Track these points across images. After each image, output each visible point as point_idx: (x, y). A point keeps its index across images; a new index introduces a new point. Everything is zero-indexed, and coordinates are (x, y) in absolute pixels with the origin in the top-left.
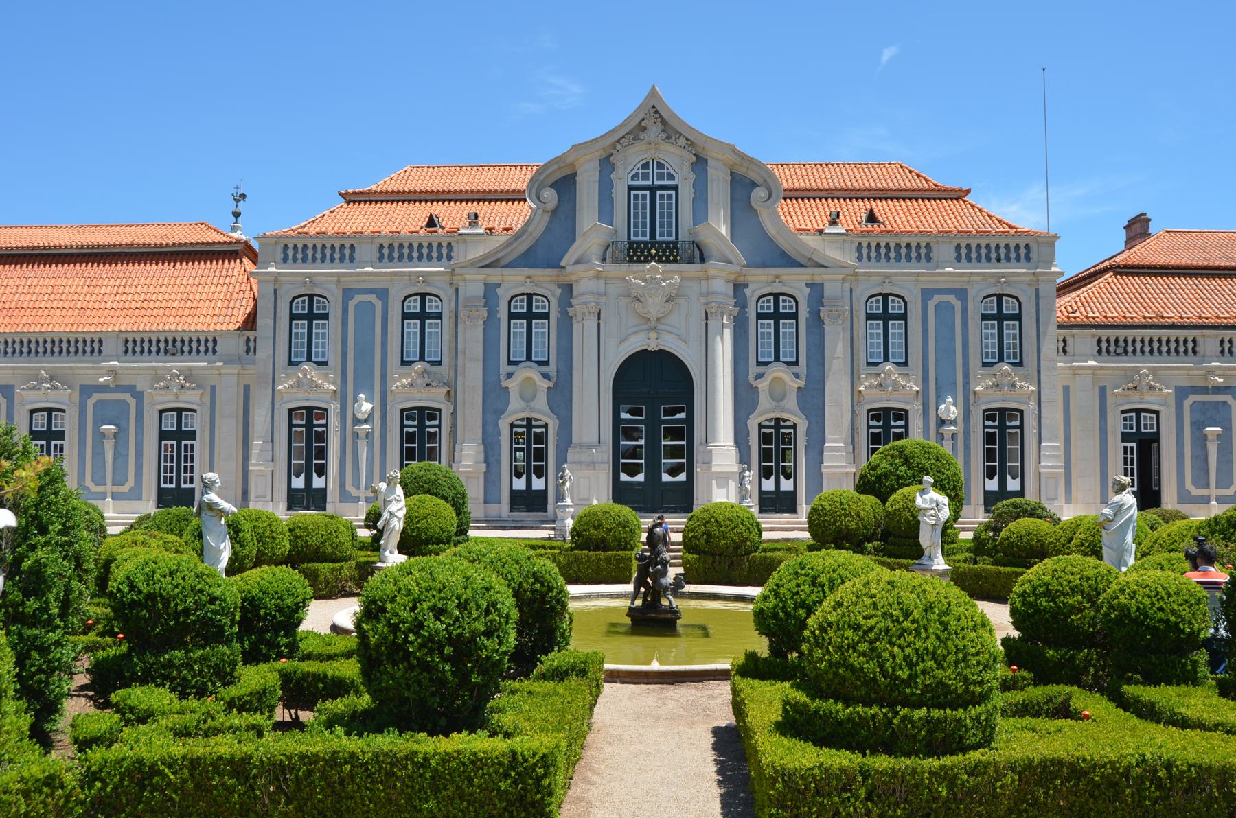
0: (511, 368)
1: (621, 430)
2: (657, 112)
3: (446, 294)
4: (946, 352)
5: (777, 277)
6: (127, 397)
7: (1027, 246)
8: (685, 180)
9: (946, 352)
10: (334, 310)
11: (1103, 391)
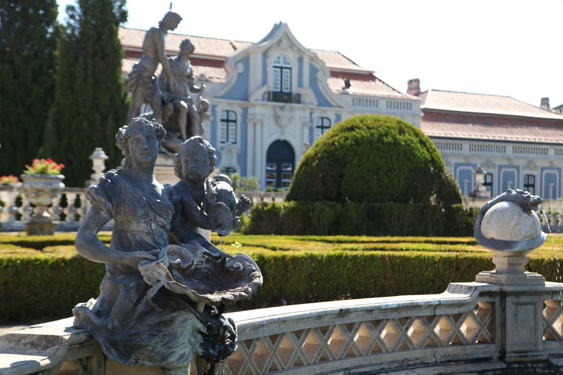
0: (222, 145)
1: (269, 174)
7: (411, 104)
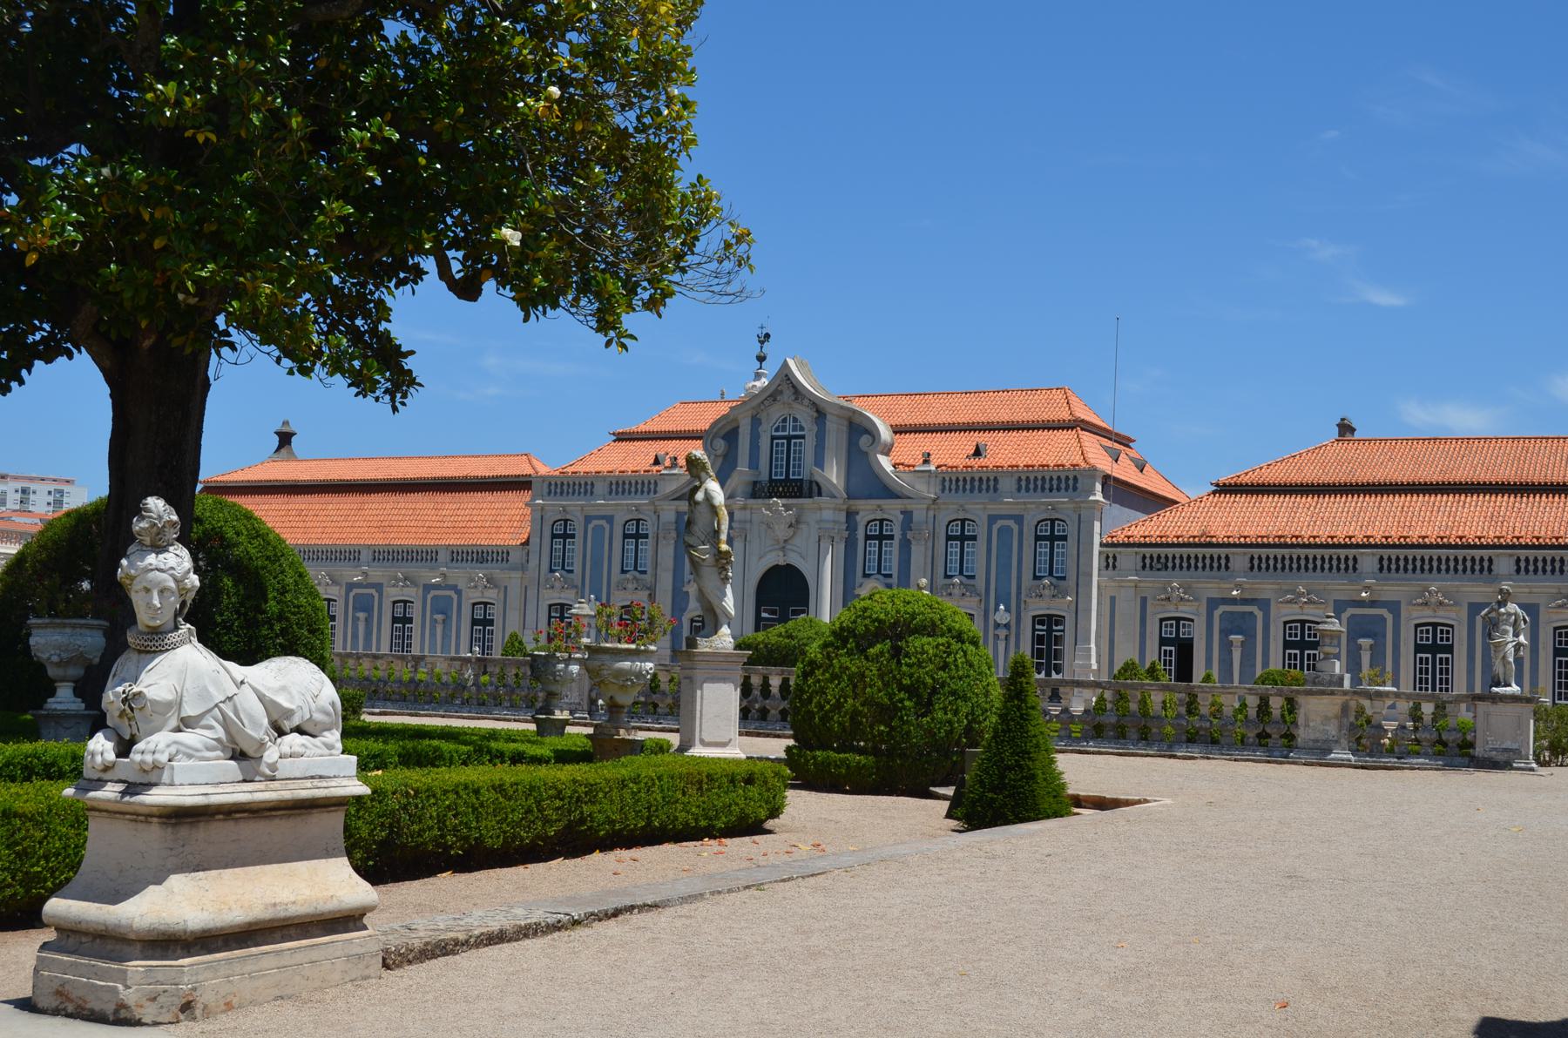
2: (789, 379)
4: (1004, 568)
5: (879, 506)
6: (452, 593)
8: (810, 431)
9: (1004, 568)
10: (579, 534)
11: (1144, 600)
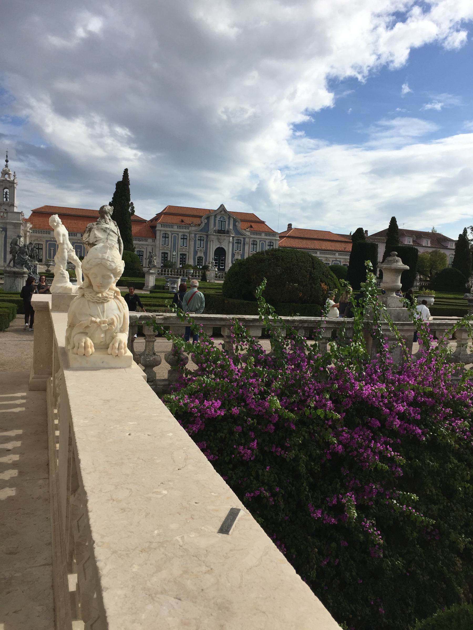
3: (188, 235)
